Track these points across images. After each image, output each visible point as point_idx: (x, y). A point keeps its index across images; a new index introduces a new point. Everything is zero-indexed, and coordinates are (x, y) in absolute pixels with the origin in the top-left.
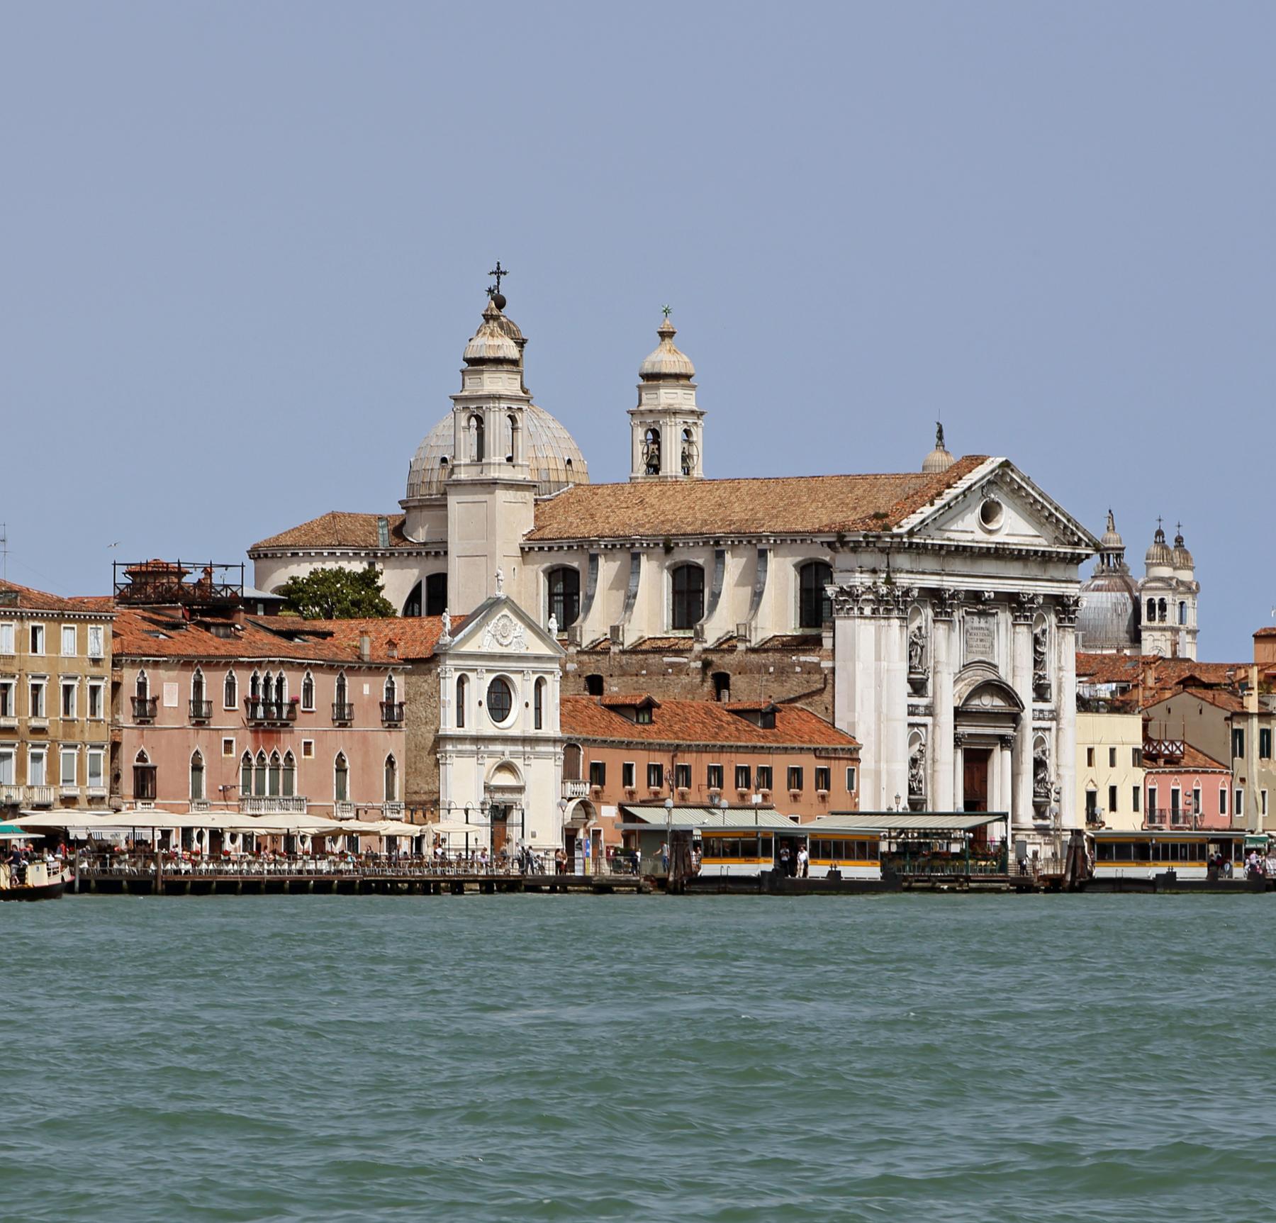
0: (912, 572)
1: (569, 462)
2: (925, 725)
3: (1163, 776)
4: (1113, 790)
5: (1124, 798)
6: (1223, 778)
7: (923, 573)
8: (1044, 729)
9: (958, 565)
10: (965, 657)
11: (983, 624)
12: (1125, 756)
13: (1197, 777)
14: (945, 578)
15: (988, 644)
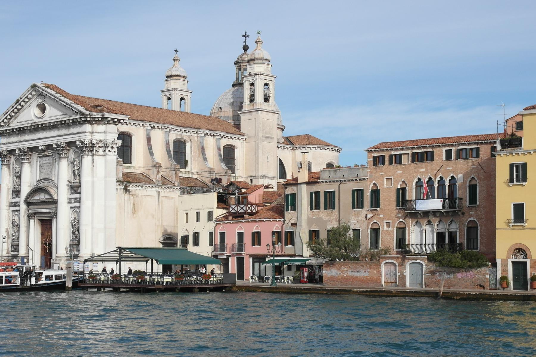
0: (4, 144)
1: (221, 108)
2: (19, 210)
3: (229, 225)
4: (196, 236)
5: (204, 239)
6: (277, 224)
7: (10, 143)
8: (77, 207)
9: (27, 137)
10: (39, 177)
11: (48, 161)
12: (204, 216)
13: (257, 224)
14: (20, 143)
15: (50, 170)
